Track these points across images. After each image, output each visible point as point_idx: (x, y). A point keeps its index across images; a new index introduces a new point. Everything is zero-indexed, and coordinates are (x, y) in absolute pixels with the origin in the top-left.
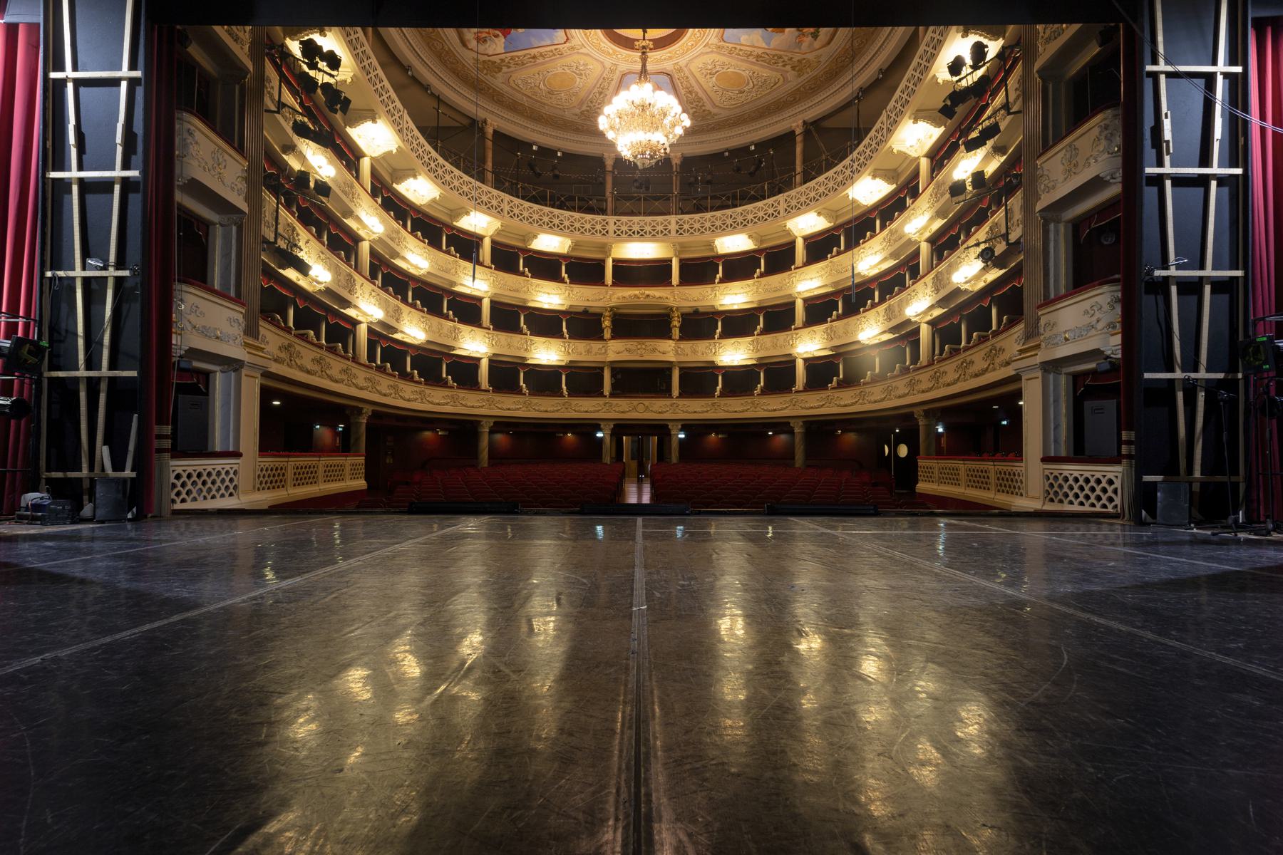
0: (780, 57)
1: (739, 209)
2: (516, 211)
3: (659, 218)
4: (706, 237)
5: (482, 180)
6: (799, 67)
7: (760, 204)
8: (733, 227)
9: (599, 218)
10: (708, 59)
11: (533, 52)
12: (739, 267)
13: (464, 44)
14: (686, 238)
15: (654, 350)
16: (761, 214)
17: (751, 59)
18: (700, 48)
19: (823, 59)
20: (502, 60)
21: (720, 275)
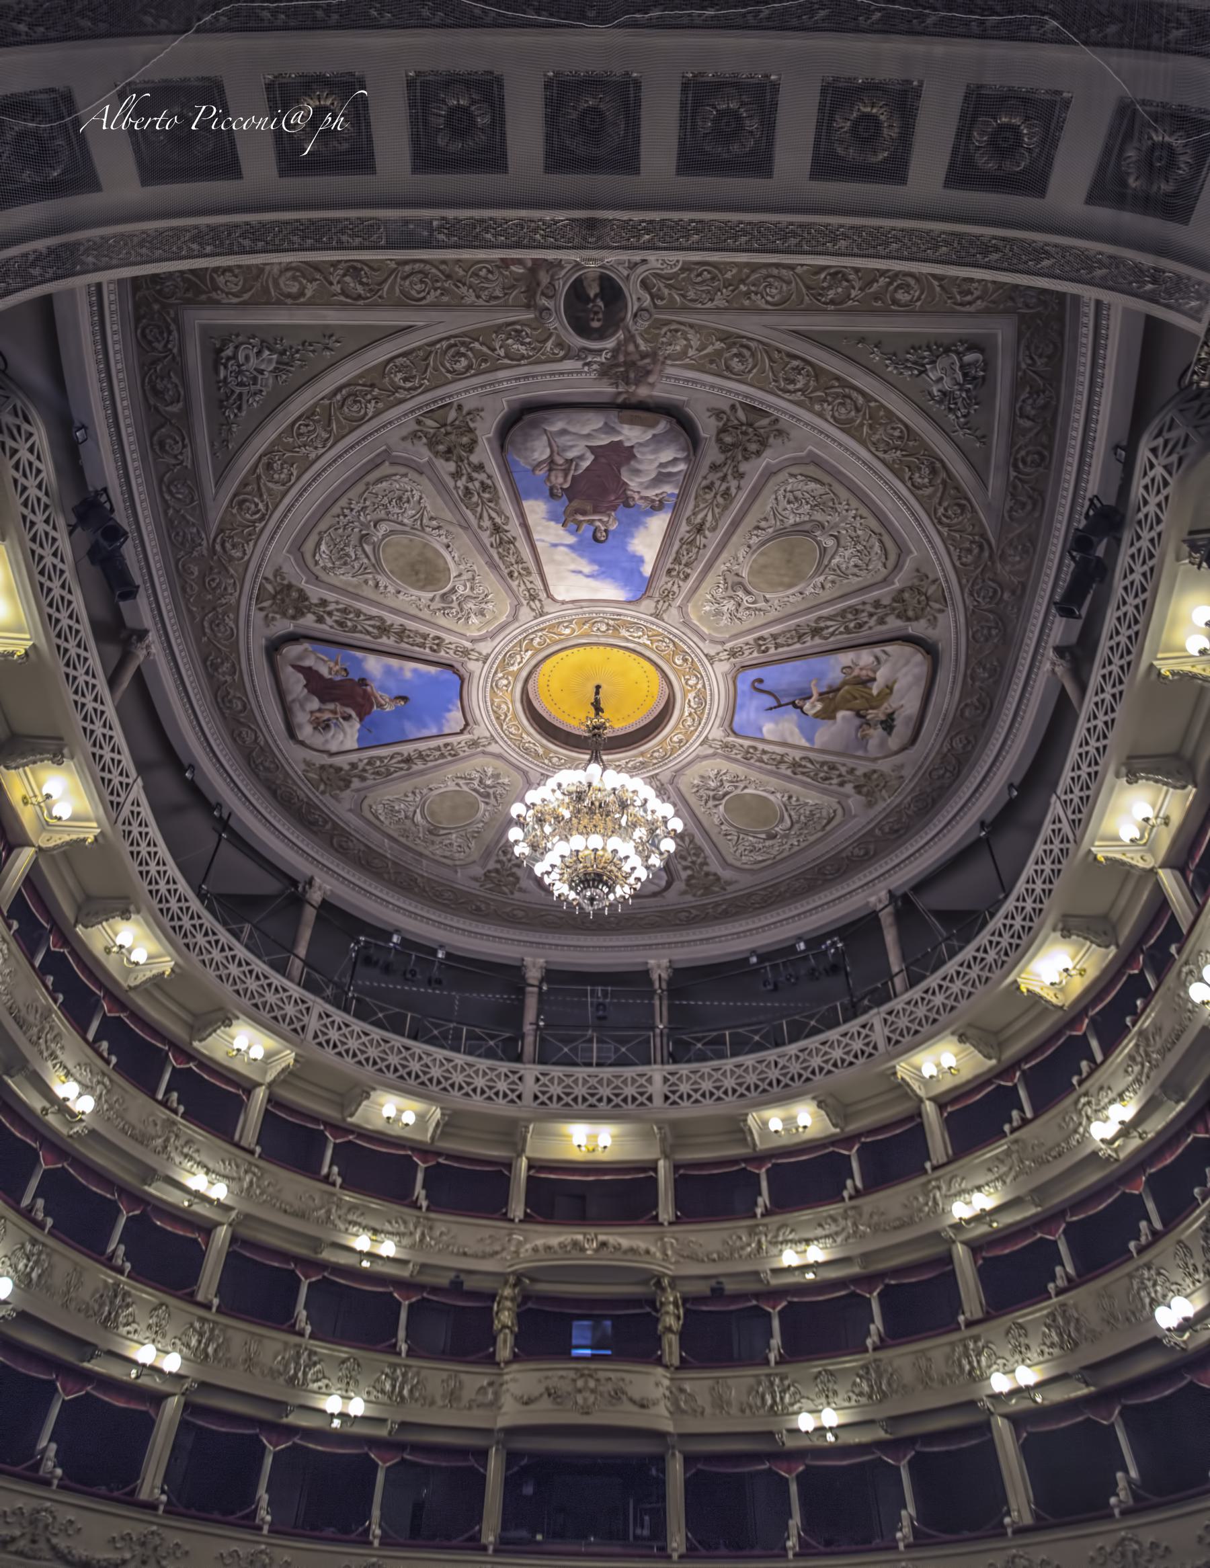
0: (833, 767)
1: (792, 1049)
2: (334, 1035)
3: (629, 1072)
4: (730, 1106)
5: (281, 968)
7: (833, 1035)
8: (782, 1091)
9: (504, 1067)
10: (710, 767)
11: (407, 749)
12: (805, 1179)
13: (291, 733)
14: (686, 1111)
15: (617, 1395)
16: (837, 1054)
17: (783, 769)
18: (694, 748)
20: (353, 766)
21: (764, 1200)
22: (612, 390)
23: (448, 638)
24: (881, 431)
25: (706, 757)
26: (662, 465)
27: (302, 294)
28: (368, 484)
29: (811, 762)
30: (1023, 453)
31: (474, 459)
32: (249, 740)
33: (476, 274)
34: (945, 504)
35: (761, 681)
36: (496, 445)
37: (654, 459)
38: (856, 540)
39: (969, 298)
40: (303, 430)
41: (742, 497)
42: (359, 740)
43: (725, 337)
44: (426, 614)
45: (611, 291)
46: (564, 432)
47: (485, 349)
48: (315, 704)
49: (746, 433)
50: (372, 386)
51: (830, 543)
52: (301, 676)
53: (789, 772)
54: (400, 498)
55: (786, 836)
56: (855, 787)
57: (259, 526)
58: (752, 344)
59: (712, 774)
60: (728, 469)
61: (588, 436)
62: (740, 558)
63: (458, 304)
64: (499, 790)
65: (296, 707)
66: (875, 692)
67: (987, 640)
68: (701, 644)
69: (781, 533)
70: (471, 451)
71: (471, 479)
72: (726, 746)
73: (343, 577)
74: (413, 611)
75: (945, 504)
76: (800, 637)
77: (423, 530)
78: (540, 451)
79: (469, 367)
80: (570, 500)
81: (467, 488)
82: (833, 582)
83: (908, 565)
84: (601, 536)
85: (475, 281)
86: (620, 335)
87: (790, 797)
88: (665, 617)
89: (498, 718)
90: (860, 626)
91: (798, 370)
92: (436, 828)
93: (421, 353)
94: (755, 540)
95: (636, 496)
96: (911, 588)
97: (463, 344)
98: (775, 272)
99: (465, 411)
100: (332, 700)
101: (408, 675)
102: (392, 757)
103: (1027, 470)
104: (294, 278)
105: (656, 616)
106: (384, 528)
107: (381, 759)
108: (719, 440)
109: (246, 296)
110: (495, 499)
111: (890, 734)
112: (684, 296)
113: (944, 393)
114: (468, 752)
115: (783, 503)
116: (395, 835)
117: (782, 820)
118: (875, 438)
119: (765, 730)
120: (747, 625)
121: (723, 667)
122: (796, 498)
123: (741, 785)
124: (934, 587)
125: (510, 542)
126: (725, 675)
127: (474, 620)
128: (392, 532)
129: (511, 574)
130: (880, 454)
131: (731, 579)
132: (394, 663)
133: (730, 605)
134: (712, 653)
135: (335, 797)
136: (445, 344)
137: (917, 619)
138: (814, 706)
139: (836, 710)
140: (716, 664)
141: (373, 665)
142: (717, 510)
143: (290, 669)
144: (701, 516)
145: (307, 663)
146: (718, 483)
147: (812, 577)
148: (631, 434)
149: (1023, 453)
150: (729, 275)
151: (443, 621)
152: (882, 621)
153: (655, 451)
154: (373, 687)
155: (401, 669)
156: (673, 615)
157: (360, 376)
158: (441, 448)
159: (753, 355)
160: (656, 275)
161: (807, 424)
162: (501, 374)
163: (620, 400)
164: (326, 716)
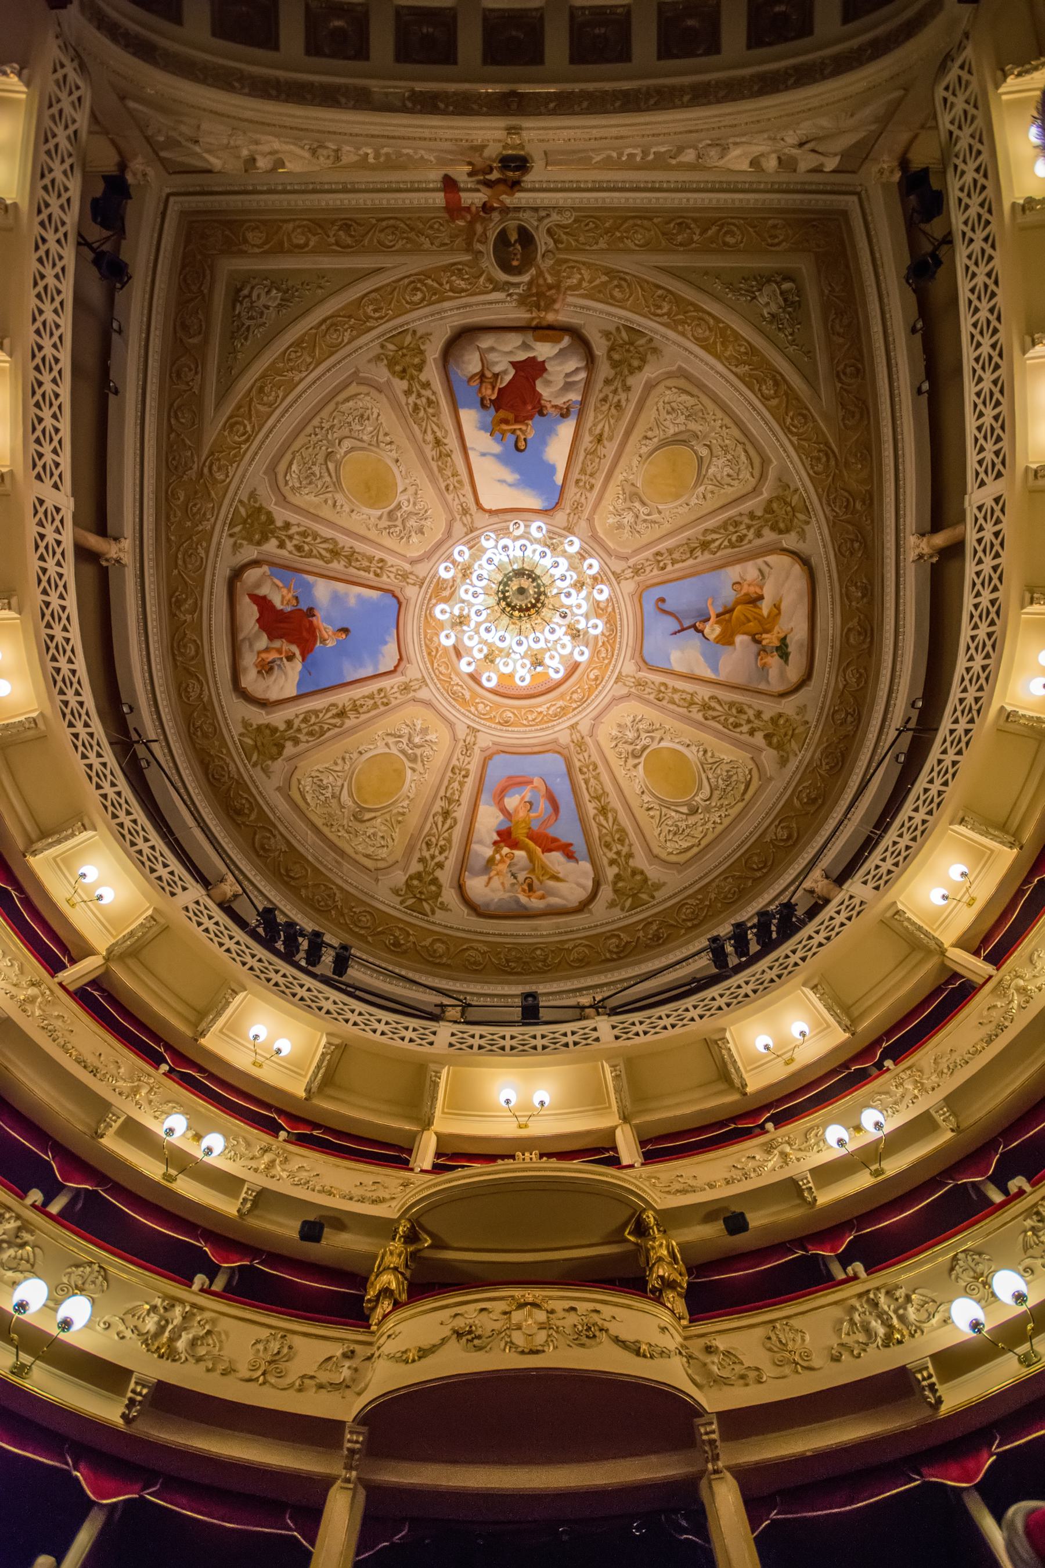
6: (779, 735)
18: (610, 688)
19: (812, 716)
22: (528, 315)
23: (391, 560)
24: (731, 348)
25: (622, 698)
26: (567, 375)
27: (306, 245)
28: (337, 404)
29: (719, 702)
31: (423, 377)
32: (194, 695)
33: (431, 227)
35: (663, 600)
36: (440, 364)
37: (561, 372)
38: (725, 449)
39: (776, 241)
40: (293, 355)
41: (632, 406)
42: (299, 685)
43: (609, 272)
44: (372, 534)
45: (526, 238)
46: (492, 349)
47: (436, 285)
48: (263, 642)
49: (630, 351)
50: (350, 317)
51: (704, 452)
52: (255, 608)
53: (699, 717)
54: (362, 416)
56: (767, 737)
57: (244, 447)
58: (628, 277)
59: (628, 721)
60: (618, 383)
61: (511, 352)
62: (633, 469)
63: (417, 249)
64: (427, 751)
66: (765, 612)
67: (852, 554)
70: (420, 370)
71: (419, 396)
72: (640, 684)
73: (306, 499)
76: (692, 552)
77: (378, 446)
78: (472, 364)
79: (423, 299)
81: (416, 404)
82: (712, 492)
83: (772, 473)
85: (431, 232)
86: (533, 271)
87: (705, 752)
89: (429, 654)
90: (741, 539)
91: (663, 298)
93: (389, 289)
94: (644, 450)
95: (549, 405)
96: (777, 498)
97: (420, 281)
98: (639, 222)
99: (419, 334)
101: (352, 602)
102: (328, 710)
104: (303, 234)
106: (347, 444)
107: (316, 713)
108: (610, 358)
109: (266, 247)
111: (786, 661)
112: (577, 241)
113: (773, 316)
114: (401, 698)
115: (663, 413)
116: (319, 822)
117: (700, 788)
118: (727, 354)
119: (672, 658)
120: (646, 539)
123: (657, 735)
124: (796, 497)
127: (415, 539)
128: (352, 449)
130: (734, 369)
131: (628, 489)
132: (340, 587)
133: (629, 517)
135: (265, 770)
136: (406, 281)
137: (787, 531)
139: (733, 635)
141: (322, 591)
142: (612, 421)
143: (247, 599)
144: (600, 427)
145: (264, 591)
146: (611, 396)
147: (695, 486)
148: (544, 351)
150: (607, 225)
151: (388, 542)
153: (561, 364)
154: (319, 620)
155: (347, 594)
157: (342, 309)
158: (398, 368)
159: (629, 286)
160: (557, 225)
161: (674, 343)
162: (446, 305)
163: (534, 323)
164: (272, 656)
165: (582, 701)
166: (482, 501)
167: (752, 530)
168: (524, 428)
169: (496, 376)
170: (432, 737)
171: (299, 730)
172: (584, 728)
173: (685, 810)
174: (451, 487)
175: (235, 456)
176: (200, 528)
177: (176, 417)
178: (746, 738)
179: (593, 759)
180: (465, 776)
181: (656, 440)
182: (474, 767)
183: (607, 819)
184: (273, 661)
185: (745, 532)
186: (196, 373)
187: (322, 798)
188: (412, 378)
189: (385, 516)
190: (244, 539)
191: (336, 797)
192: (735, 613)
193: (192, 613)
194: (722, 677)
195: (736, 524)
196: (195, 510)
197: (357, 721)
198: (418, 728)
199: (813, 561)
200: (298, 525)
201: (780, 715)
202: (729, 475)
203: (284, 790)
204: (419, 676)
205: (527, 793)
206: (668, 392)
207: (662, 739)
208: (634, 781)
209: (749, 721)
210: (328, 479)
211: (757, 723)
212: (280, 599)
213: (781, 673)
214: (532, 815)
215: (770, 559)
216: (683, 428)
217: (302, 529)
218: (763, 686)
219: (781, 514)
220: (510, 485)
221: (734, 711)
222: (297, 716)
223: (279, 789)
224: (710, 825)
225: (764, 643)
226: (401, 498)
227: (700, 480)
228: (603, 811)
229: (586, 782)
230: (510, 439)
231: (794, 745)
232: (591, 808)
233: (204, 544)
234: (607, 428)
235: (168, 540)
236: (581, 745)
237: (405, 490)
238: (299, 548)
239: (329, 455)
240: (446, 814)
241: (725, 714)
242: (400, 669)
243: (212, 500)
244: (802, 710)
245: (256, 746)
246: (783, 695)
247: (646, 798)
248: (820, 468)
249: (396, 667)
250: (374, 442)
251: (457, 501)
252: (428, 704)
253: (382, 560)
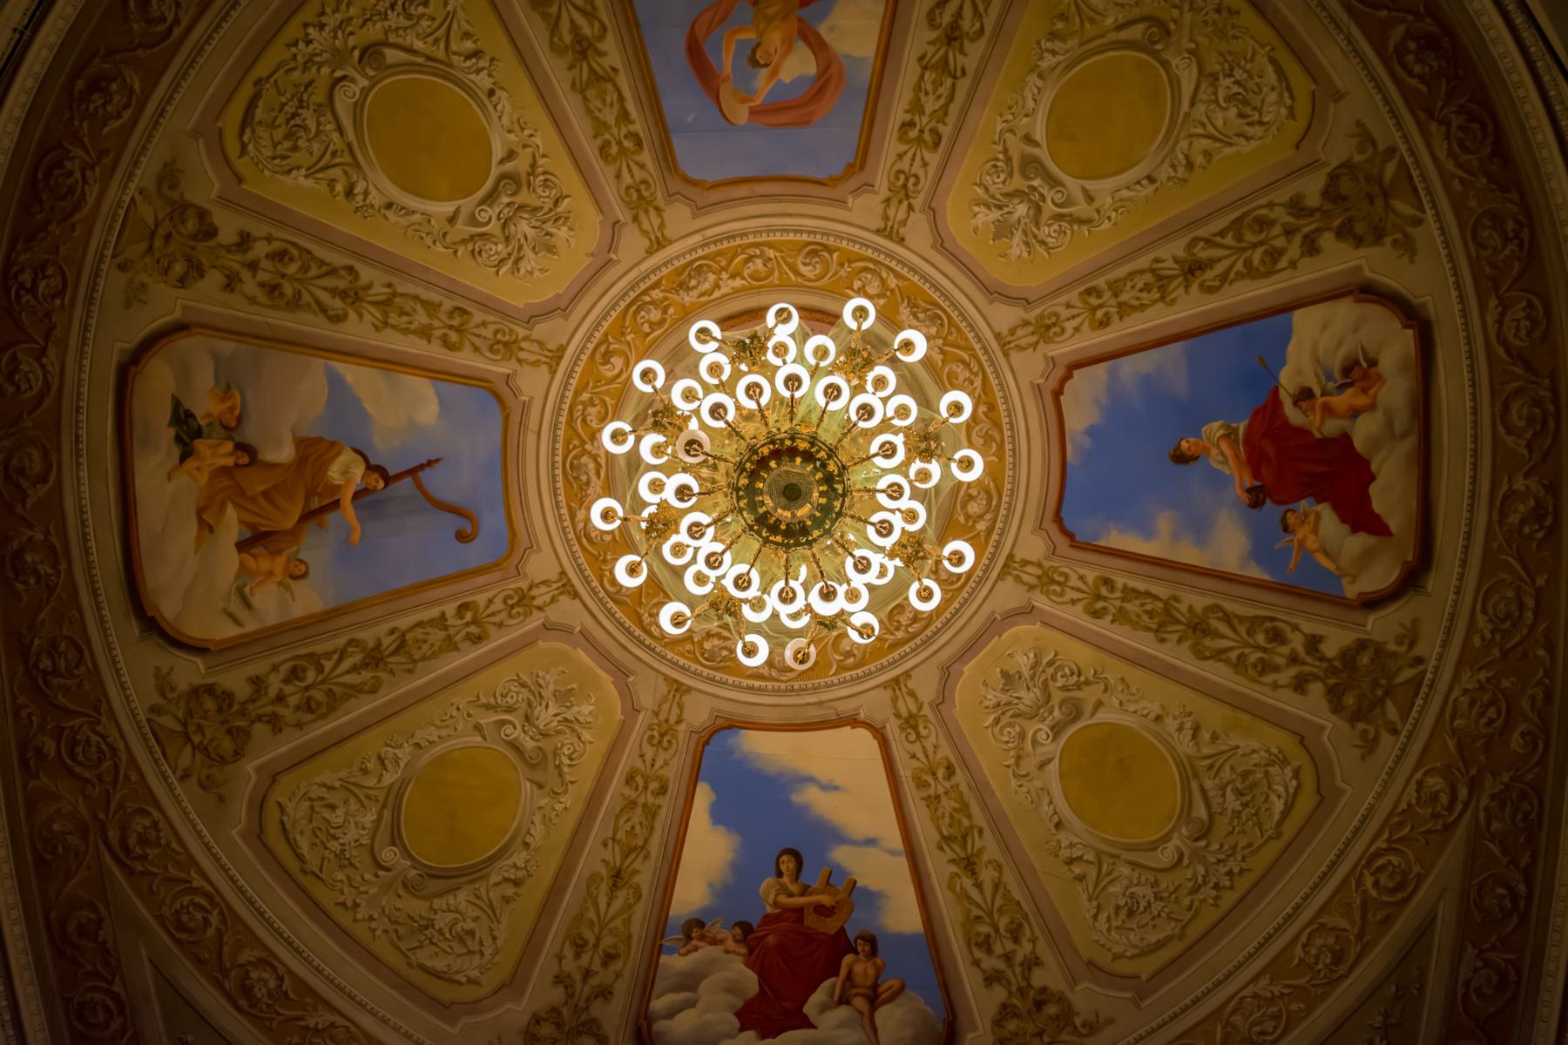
6: (183, 238)
18: (576, 334)
23: (1075, 615)
26: (692, 1004)
28: (1182, 936)
29: (323, 309)
30: (116, 1024)
31: (999, 994)
32: (1518, 311)
34: (211, 932)
35: (462, 537)
40: (1269, 1026)
44: (1115, 670)
48: (1363, 432)
51: (388, 854)
52: (1377, 506)
53: (366, 273)
54: (1131, 914)
55: (339, 58)
56: (212, 232)
59: (531, 261)
62: (542, 819)
64: (997, 184)
65: (1402, 419)
66: (231, 513)
67: (53, 644)
68: (589, 622)
69: (475, 872)
70: (1004, 1006)
71: (1008, 958)
72: (506, 347)
74: (1137, 676)
75: (211, 932)
76: (401, 646)
77: (1099, 855)
80: (842, 930)
81: (1016, 940)
82: (365, 771)
83: (241, 809)
84: (787, 864)
87: (349, 193)
88: (663, 688)
90: (295, 674)
92: (1146, 46)
94: (519, 858)
95: (731, 944)
96: (223, 761)
100: (1325, 442)
101: (1164, 523)
102: (1224, 277)
103: (98, 996)
105: (679, 689)
106: (1165, 857)
107: (1251, 273)
110: (971, 921)
111: (177, 404)
114: (1057, 305)
117: (357, 107)
119: (434, 408)
121: (540, 566)
122: (462, 941)
123: (462, 229)
125: (947, 839)
126: (532, 546)
127: (1023, 662)
128: (1153, 847)
129: (950, 770)
132: (1189, 554)
133: (546, 716)
134: (564, 599)
135: (1366, 139)
137: (195, 692)
138: (345, 472)
139: (301, 462)
140: (553, 574)
141: (1230, 544)
142: (591, 914)
143: (1393, 524)
144: (618, 903)
145: (1357, 543)
146: (596, 966)
147: (403, 784)
149: (116, 1024)
151: (1082, 655)
152: (258, 683)
154: (1240, 480)
156: (649, 693)
158: (1051, 1009)
164: (1342, 401)
165: (638, 305)
166: (875, 744)
167: (272, 692)
168: (783, 899)
169: (844, 1000)
170: (986, 217)
171: (1289, 232)
172: (632, 243)
173: (392, 56)
174: (941, 773)
175: (1401, 824)
176: (1483, 675)
177: (1514, 896)
178: (259, 229)
179: (611, 171)
180: (911, 124)
181: (494, 879)
182: (889, 148)
183: (575, 28)
184: (1342, 387)
185: (288, 689)
186: (1467, 984)
187: (1239, 75)
188: (1022, 992)
189: (1088, 708)
190: (1394, 655)
191: (1208, 77)
192: (297, 512)
193: (1510, 495)
194: (319, 364)
195: (308, 706)
196: (1492, 712)
197: (1161, 253)
198: (1018, 235)
199: (134, 628)
200: (1275, 686)
201: (182, 282)
202: (332, 807)
203: (1326, 93)
204: (1015, 357)
205: (762, 85)
206: (476, 973)
207: (452, 220)
208: (513, 123)
209: (253, 266)
210: (1208, 784)
211: (234, 262)
212: (1323, 525)
213: (185, 377)
214: (751, 36)
215: (231, 631)
216: (437, 903)
217: (1269, 679)
218: (227, 347)
219: (215, 726)
220: (811, 780)
221: (288, 289)
222: (1293, 264)
223: (1338, 96)
224: (332, 20)
225: (229, 446)
226: (1050, 748)
227: (393, 800)
228: (583, 48)
229: (624, 116)
230: (813, 875)
231: (146, 212)
232: (612, 52)
233: (1477, 641)
234: (603, 901)
235: (1551, 649)
236: (639, 202)
237: (1042, 766)
238: (1277, 637)
239: (1204, 832)
240: (953, 36)
241: (308, 282)
242: (1060, 372)
243: (1454, 732)
244: (135, 296)
245: (1386, 196)
246: (180, 328)
247: (484, 81)
248: (140, 824)
249: (1068, 376)
250: (1107, 862)
251: (929, 744)
252: (995, 293)
253: (1097, 615)
